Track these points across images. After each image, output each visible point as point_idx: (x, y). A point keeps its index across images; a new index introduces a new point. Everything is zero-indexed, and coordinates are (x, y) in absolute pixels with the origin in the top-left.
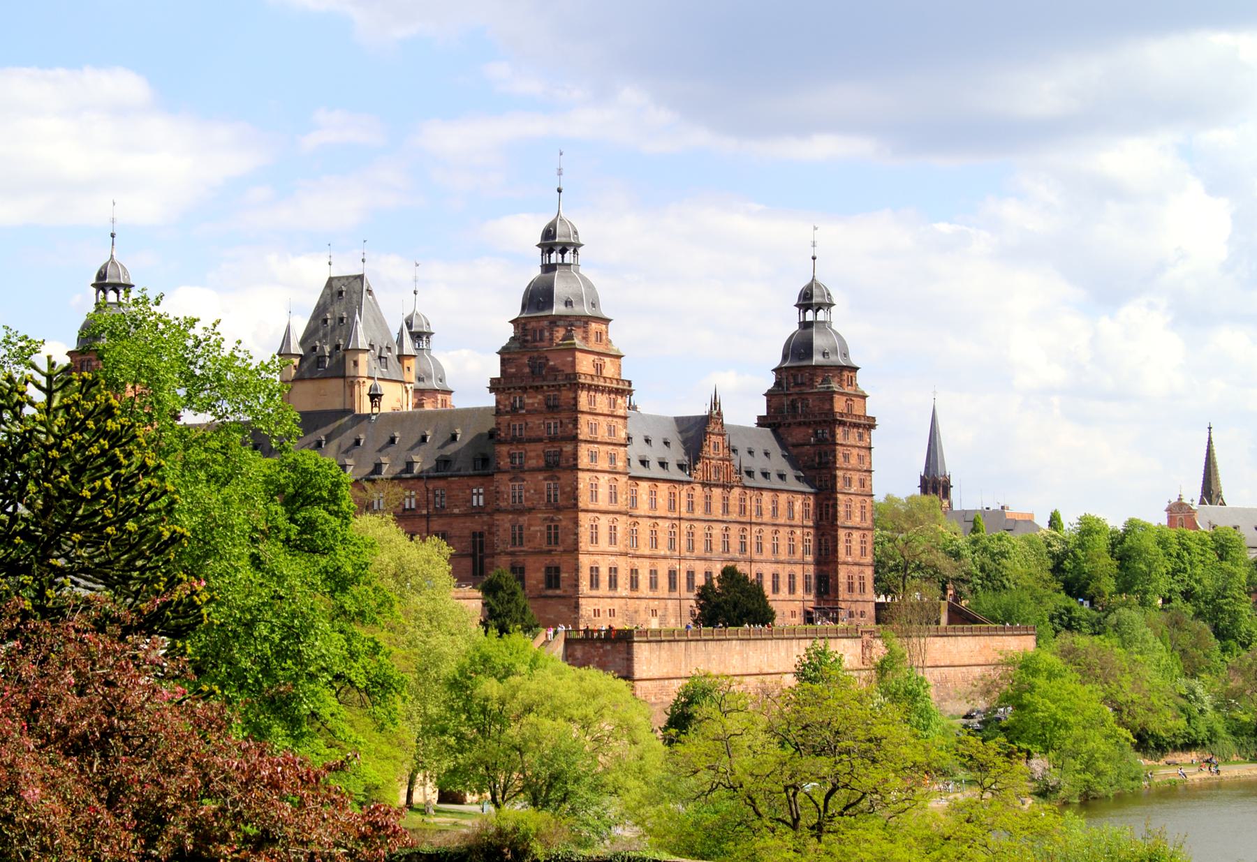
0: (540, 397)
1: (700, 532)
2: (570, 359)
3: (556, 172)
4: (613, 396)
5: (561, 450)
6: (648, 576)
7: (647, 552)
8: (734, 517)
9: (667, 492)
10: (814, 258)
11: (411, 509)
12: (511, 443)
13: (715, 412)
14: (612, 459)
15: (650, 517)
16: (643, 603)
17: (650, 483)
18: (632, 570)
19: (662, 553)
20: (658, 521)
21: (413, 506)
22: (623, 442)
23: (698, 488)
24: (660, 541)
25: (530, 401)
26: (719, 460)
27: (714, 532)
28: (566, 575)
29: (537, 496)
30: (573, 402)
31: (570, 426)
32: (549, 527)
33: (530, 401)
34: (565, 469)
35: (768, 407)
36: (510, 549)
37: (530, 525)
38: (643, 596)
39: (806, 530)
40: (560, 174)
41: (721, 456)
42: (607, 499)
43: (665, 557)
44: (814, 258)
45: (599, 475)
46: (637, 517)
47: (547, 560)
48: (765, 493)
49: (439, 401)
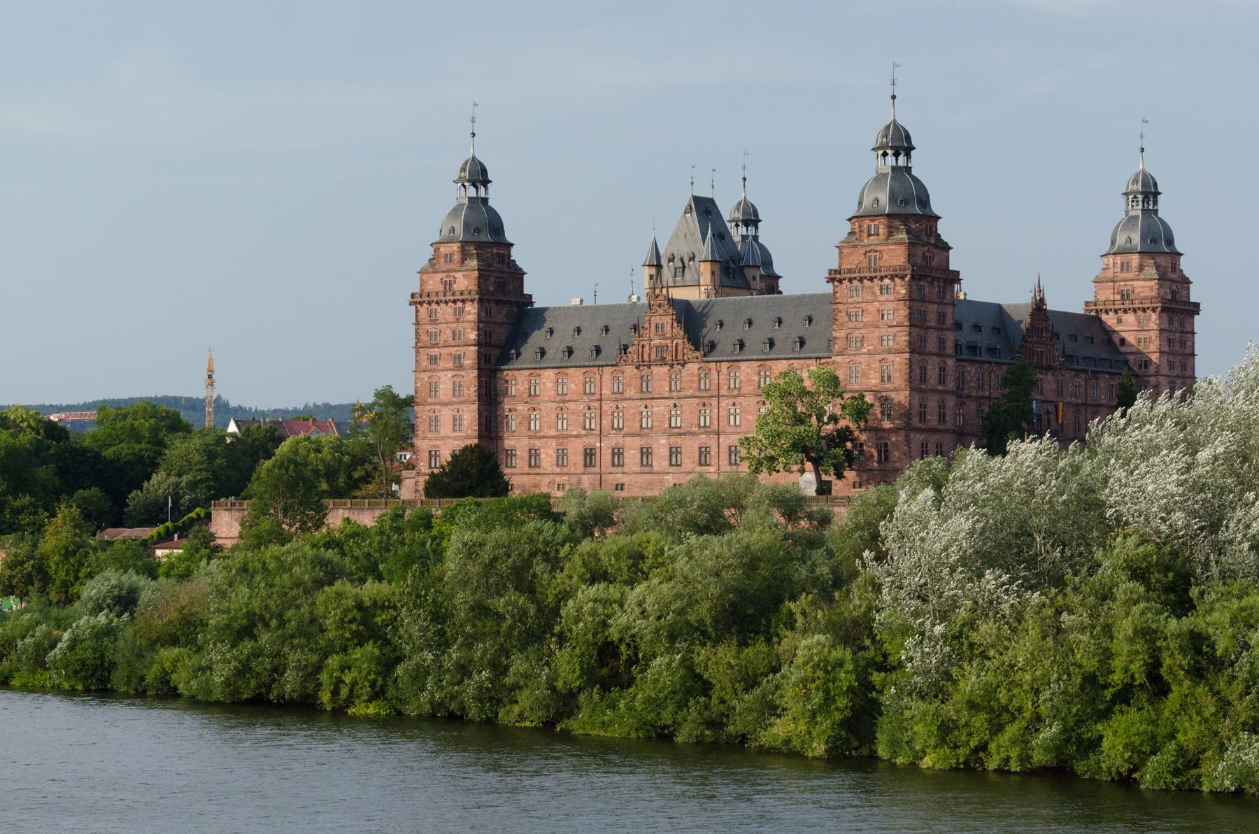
1: (632, 411)
3: (470, 119)
4: (460, 304)
6: (555, 455)
7: (553, 432)
8: (689, 392)
9: (581, 378)
10: (894, 97)
14: (457, 359)
16: (546, 480)
17: (556, 371)
18: (530, 450)
19: (575, 433)
20: (567, 405)
22: (474, 343)
23: (630, 370)
38: (546, 472)
40: (473, 122)
41: (669, 335)
42: (451, 393)
43: (578, 436)
44: (894, 97)
45: (441, 374)
48: (744, 365)
49: (1119, 265)
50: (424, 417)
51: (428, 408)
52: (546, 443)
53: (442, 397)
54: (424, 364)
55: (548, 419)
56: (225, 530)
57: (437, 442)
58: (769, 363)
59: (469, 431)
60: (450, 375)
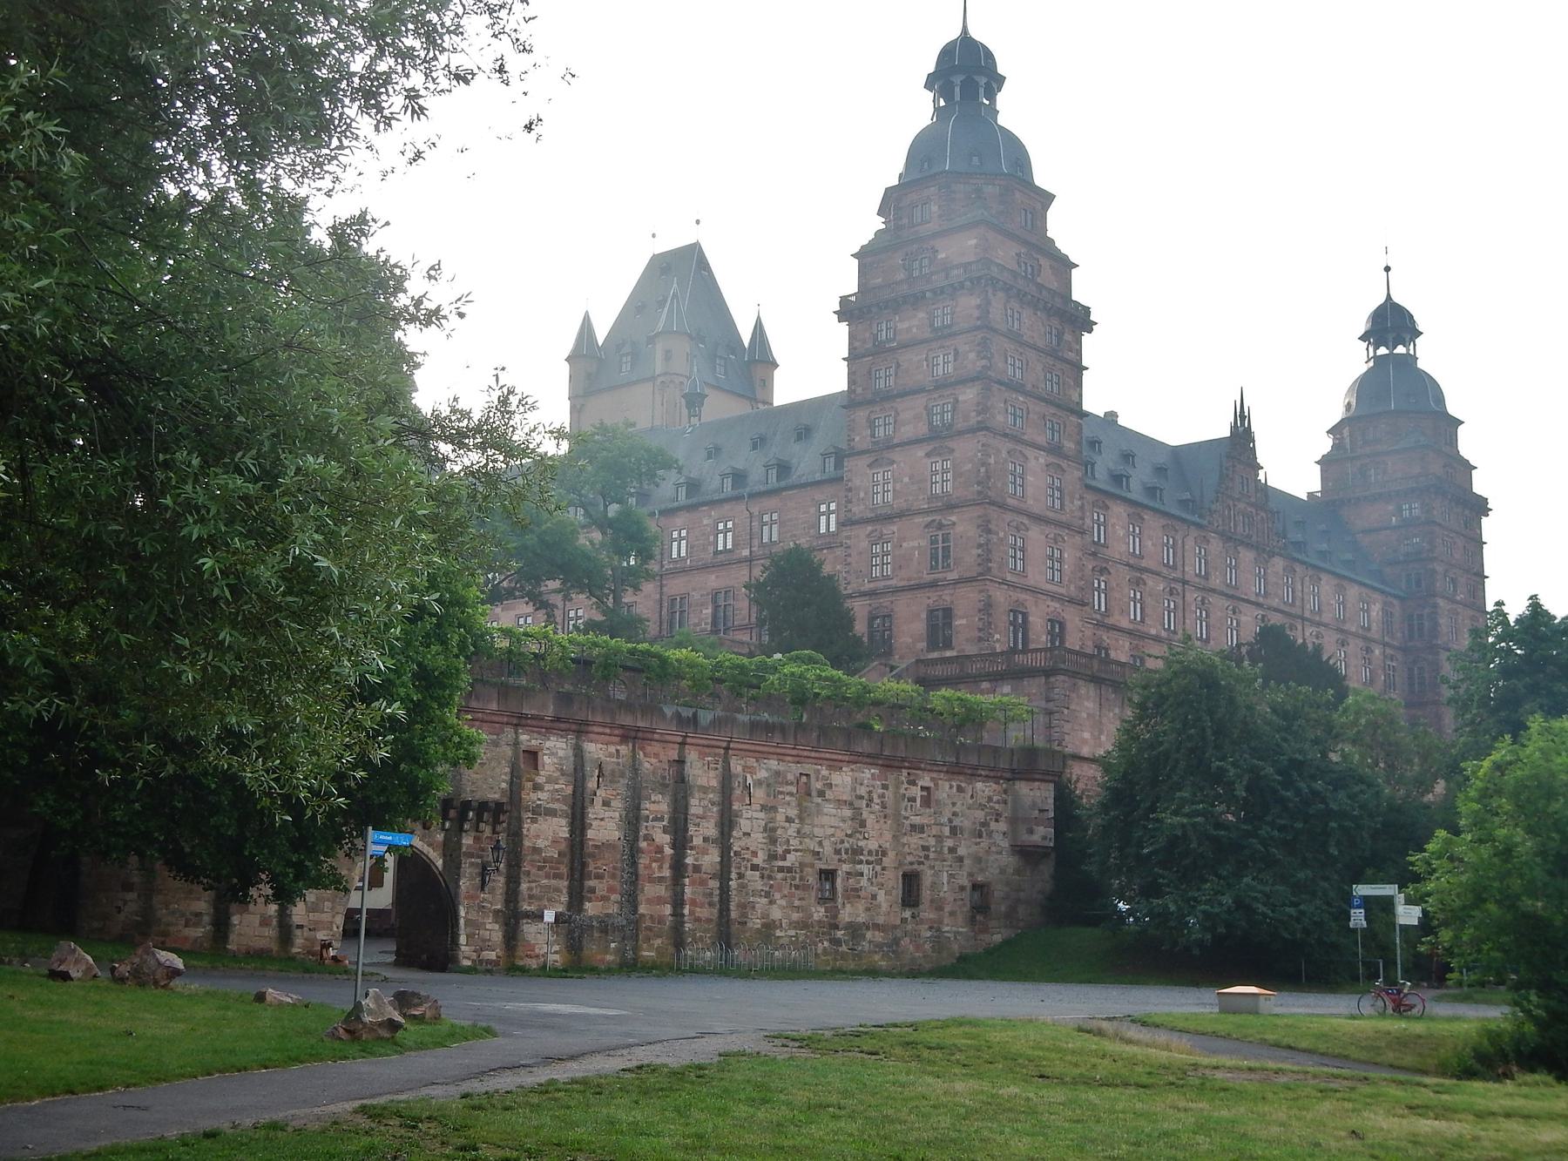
0: (921, 315)
2: (973, 242)
5: (957, 401)
7: (1125, 624)
10: (1387, 269)
11: (726, 550)
12: (871, 402)
13: (1241, 429)
15: (1128, 565)
19: (1153, 632)
21: (729, 546)
24: (1148, 611)
25: (906, 325)
26: (1252, 505)
27: (1243, 619)
28: (964, 622)
29: (915, 487)
30: (976, 313)
31: (972, 356)
32: (933, 542)
33: (906, 325)
34: (960, 433)
35: (1324, 479)
36: (867, 587)
37: (904, 539)
39: (1389, 651)
44: (1387, 269)
45: (1030, 452)
46: (1107, 561)
47: (927, 599)
48: (1324, 577)
50: (1001, 534)
51: (1008, 517)
52: (1117, 640)
53: (1030, 502)
54: (1000, 418)
55: (1117, 595)
56: (1087, 735)
57: (1023, 596)
58: (1345, 583)
59: (1072, 588)
60: (1042, 460)
